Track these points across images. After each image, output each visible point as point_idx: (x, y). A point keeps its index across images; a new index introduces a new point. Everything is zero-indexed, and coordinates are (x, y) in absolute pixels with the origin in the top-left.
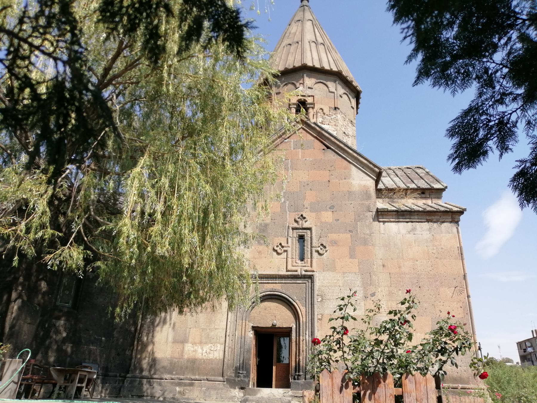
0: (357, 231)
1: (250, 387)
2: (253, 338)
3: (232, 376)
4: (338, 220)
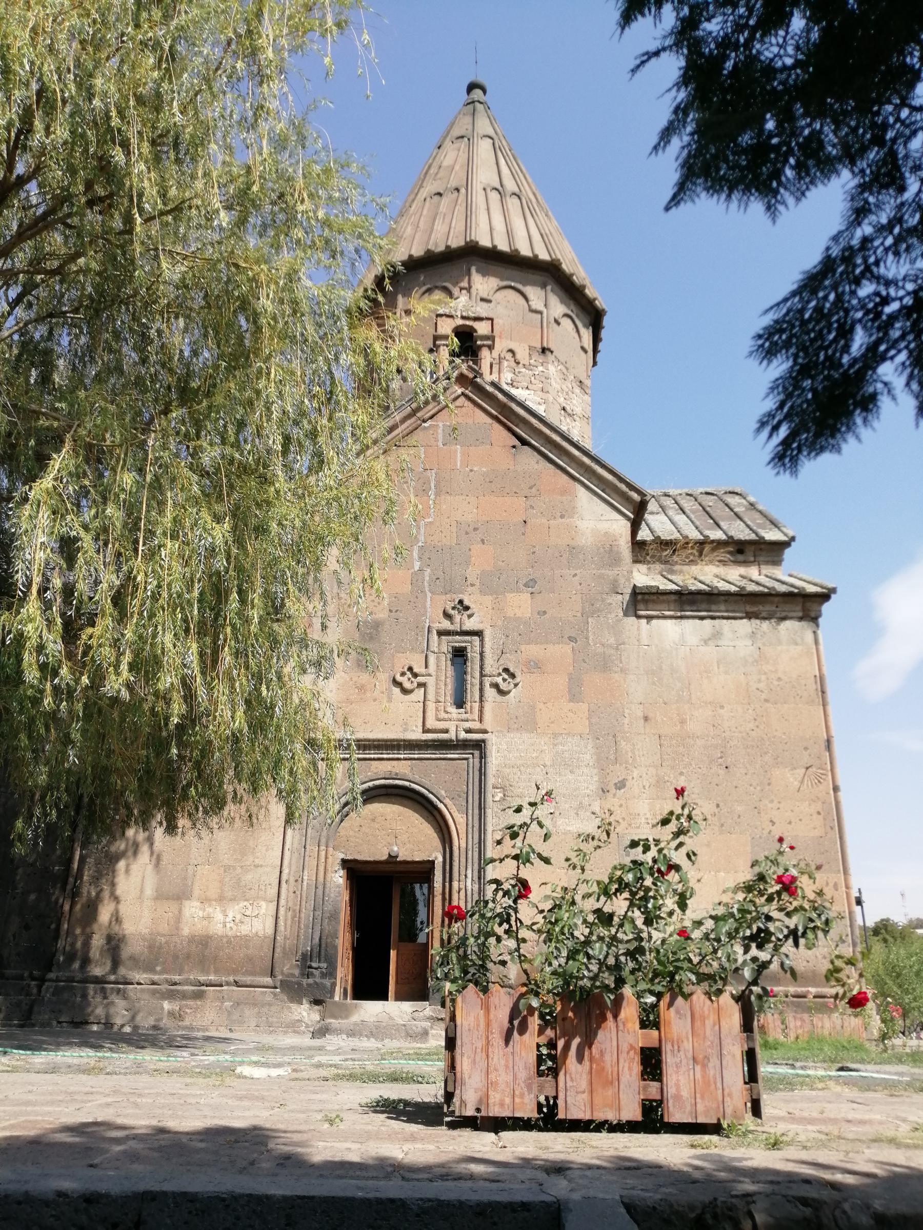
0: (587, 638)
1: (337, 998)
2: (344, 886)
3: (293, 975)
4: (545, 613)
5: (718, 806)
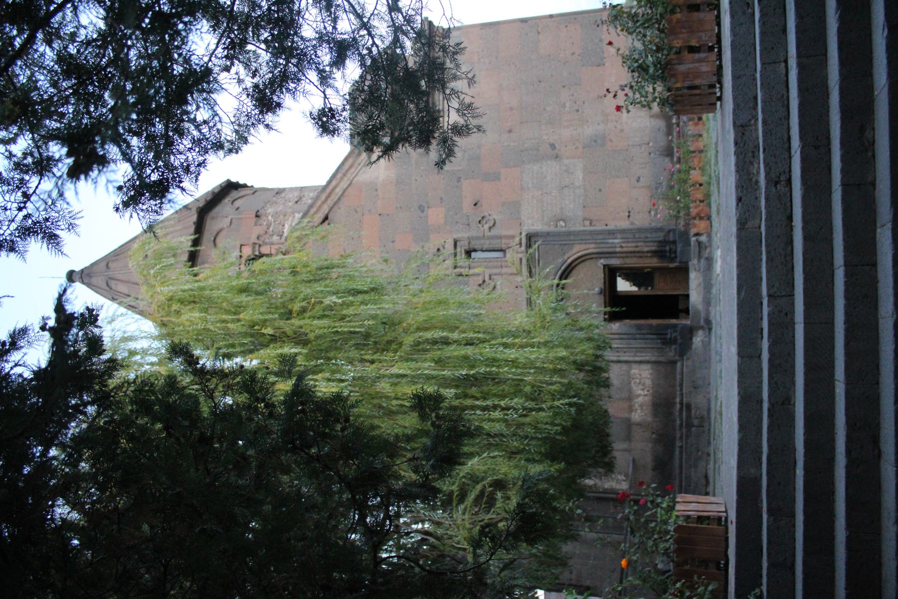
0: (458, 171)
4: (441, 199)
5: (564, 87)
